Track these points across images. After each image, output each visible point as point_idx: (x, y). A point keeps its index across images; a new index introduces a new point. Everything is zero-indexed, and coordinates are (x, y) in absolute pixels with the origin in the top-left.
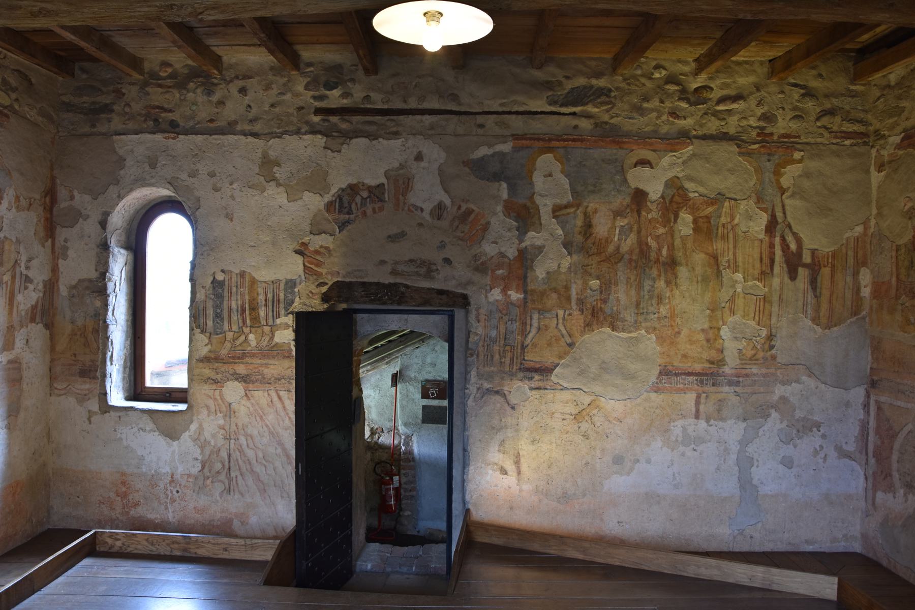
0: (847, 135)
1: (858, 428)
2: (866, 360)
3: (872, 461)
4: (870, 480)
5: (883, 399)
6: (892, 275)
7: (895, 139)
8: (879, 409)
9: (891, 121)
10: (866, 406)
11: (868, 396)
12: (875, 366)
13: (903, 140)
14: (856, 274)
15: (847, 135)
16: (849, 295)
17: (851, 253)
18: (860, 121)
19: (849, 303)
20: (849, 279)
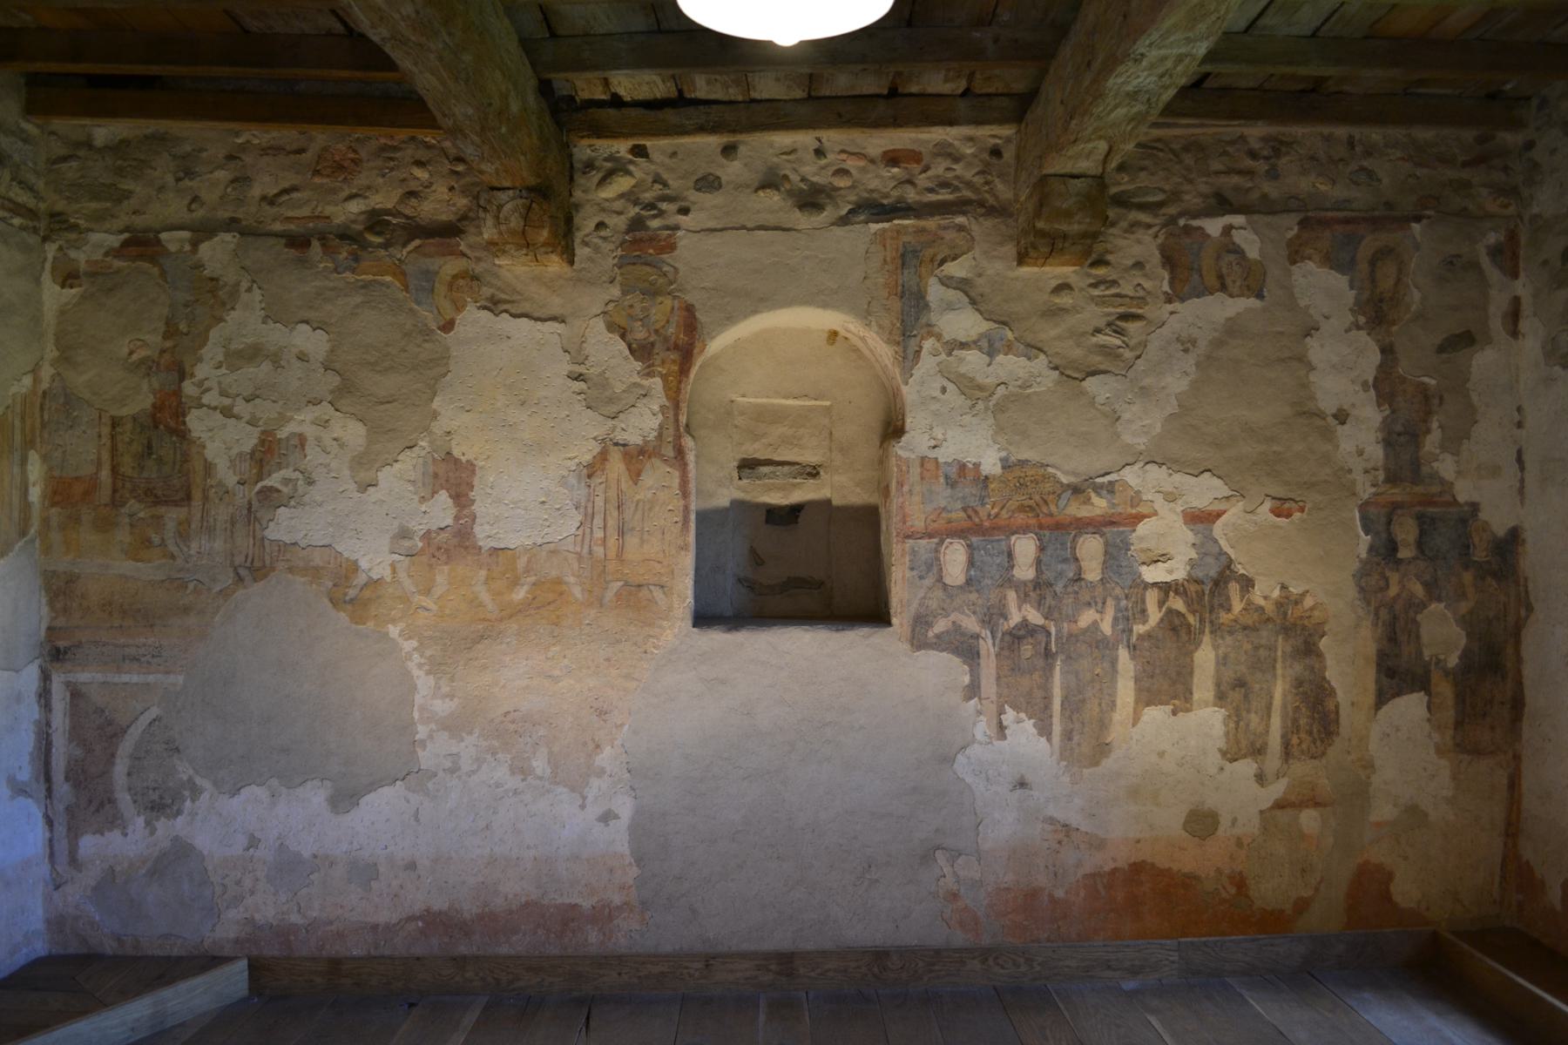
0: (17, 209)
1: (33, 736)
2: (35, 615)
3: (62, 788)
4: (61, 830)
5: (83, 677)
6: (99, 464)
7: (105, 239)
8: (76, 694)
9: (94, 205)
10: (44, 695)
11: (46, 677)
12: (61, 622)
13: (125, 244)
14: (24, 461)
15: (17, 209)
16: (16, 500)
17: (17, 423)
18: (31, 189)
19: (16, 514)
20: (16, 470)
